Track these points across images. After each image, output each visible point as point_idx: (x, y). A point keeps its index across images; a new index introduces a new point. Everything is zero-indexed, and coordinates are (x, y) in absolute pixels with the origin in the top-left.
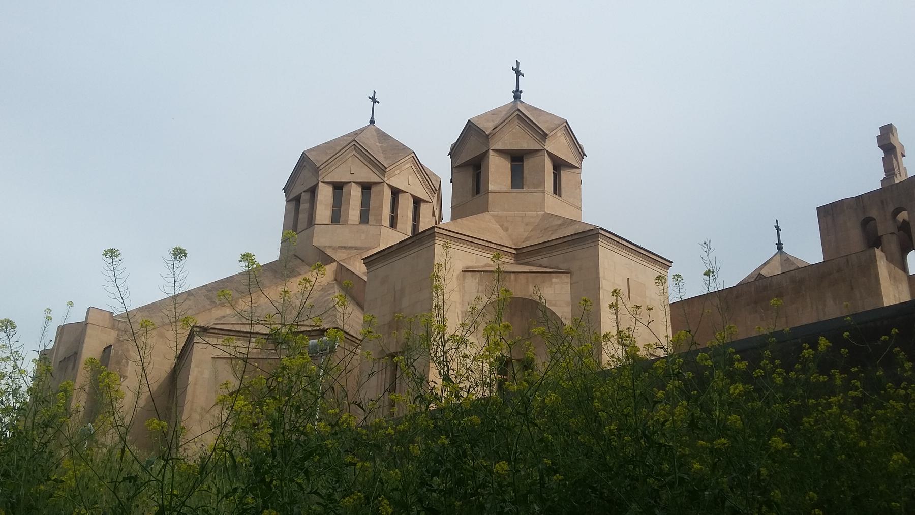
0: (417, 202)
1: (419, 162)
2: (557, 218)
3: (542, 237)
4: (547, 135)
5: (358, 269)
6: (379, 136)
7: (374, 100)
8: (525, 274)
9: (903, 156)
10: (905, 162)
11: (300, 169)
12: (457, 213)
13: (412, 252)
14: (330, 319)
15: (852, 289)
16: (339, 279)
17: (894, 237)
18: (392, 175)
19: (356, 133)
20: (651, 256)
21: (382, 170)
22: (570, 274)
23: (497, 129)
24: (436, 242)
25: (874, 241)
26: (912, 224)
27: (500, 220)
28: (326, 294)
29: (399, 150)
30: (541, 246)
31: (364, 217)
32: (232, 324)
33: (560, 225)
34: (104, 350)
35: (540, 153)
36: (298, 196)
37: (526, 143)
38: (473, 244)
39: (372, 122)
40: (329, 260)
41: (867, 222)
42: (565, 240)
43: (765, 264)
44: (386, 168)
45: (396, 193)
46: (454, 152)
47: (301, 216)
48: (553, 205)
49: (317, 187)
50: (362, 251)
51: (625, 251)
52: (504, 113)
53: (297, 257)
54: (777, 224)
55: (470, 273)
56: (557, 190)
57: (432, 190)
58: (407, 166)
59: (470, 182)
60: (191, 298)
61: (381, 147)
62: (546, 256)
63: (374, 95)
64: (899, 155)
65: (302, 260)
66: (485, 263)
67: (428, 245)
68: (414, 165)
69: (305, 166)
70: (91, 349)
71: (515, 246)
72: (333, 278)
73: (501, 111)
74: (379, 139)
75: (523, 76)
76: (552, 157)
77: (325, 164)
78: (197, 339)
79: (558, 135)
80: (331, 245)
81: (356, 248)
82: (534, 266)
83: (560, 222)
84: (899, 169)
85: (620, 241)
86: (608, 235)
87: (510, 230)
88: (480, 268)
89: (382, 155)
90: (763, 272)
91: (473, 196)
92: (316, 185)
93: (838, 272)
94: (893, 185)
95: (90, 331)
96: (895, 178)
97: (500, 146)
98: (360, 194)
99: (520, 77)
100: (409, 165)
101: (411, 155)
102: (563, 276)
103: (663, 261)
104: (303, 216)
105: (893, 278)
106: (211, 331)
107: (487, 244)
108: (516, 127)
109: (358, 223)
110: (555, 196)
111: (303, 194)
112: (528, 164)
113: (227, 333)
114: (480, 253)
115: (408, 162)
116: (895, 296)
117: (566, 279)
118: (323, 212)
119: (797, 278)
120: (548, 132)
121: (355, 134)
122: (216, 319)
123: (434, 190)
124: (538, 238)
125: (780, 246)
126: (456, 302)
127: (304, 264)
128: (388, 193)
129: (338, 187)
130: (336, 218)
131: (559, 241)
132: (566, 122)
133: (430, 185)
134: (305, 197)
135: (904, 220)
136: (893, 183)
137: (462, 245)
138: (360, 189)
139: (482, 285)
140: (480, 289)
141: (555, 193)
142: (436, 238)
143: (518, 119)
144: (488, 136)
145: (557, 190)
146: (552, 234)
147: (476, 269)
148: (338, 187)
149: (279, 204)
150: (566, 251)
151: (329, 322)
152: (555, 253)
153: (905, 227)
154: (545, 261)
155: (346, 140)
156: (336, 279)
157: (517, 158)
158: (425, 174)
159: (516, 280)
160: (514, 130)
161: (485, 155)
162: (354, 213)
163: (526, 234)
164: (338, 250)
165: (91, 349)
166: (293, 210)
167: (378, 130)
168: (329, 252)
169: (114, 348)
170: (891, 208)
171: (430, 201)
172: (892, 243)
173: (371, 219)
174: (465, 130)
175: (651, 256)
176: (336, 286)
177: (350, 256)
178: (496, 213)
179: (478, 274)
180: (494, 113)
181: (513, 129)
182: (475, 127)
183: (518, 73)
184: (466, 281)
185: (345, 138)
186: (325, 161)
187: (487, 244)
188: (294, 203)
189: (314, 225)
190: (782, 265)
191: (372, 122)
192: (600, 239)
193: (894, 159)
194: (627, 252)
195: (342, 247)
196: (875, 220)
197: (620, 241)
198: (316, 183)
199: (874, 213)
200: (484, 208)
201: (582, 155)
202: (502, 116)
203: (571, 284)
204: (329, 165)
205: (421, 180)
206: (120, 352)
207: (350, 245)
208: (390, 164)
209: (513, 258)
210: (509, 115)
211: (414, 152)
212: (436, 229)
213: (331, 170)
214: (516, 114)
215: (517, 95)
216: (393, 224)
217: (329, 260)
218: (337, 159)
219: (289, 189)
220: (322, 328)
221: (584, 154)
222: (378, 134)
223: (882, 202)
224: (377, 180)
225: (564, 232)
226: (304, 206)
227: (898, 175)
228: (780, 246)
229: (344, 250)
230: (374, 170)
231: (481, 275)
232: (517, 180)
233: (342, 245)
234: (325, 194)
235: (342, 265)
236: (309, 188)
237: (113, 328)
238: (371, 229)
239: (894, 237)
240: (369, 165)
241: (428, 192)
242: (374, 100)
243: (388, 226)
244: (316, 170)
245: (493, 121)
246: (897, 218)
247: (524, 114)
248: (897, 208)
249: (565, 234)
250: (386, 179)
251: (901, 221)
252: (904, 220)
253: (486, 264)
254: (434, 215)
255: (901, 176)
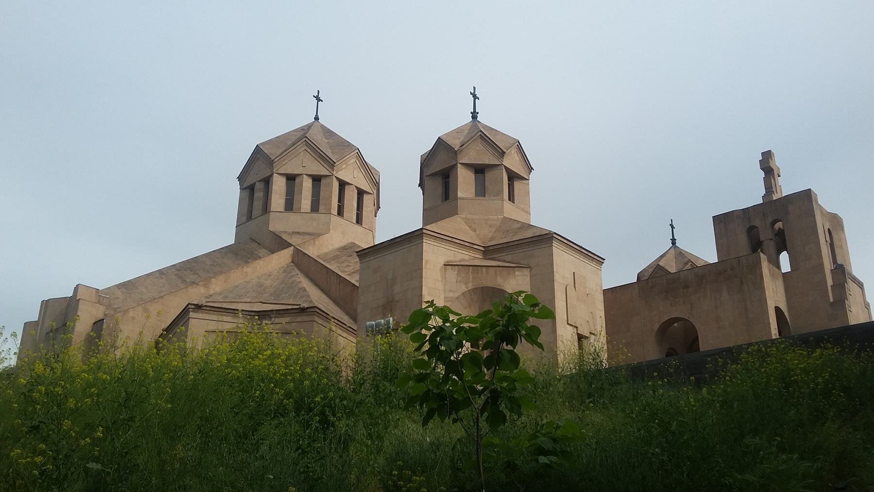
0: (361, 193)
1: (364, 159)
2: (515, 222)
3: (505, 237)
4: (504, 153)
5: (311, 252)
6: (325, 132)
7: (318, 99)
8: (494, 268)
9: (779, 176)
10: (780, 181)
11: (254, 161)
12: (430, 214)
13: (404, 247)
14: (304, 299)
15: (742, 283)
16: (296, 263)
17: (772, 242)
18: (340, 169)
19: (302, 129)
20: (590, 254)
21: (332, 165)
22: (529, 269)
23: (464, 146)
24: (424, 240)
25: (756, 246)
26: (786, 233)
27: (469, 223)
28: (290, 275)
29: (345, 147)
30: (505, 245)
31: (315, 208)
32: (221, 302)
33: (520, 228)
34: (94, 323)
35: (499, 167)
36: (252, 184)
37: (488, 159)
38: (452, 243)
39: (317, 118)
40: (285, 245)
41: (752, 231)
42: (525, 241)
43: (662, 256)
44: (335, 163)
45: (343, 184)
46: (426, 161)
47: (256, 203)
48: (510, 210)
49: (271, 179)
50: (315, 237)
51: (571, 251)
52: (466, 131)
53: (255, 241)
54: (672, 223)
55: (450, 266)
56: (511, 198)
57: (375, 184)
58: (353, 161)
59: (440, 190)
60: (163, 276)
61: (328, 143)
62: (510, 253)
63: (318, 94)
64: (776, 175)
65: (258, 243)
66: (461, 258)
67: (417, 243)
68: (359, 161)
69: (258, 158)
70: (83, 325)
71: (483, 244)
72: (290, 260)
73: (463, 130)
74: (324, 135)
75: (479, 99)
76: (507, 169)
77: (280, 157)
78: (192, 315)
79: (513, 153)
80: (285, 231)
81: (309, 234)
82: (499, 261)
83: (519, 225)
84: (776, 187)
85: (568, 243)
86: (559, 238)
87: (477, 231)
88: (456, 262)
89: (330, 150)
90: (661, 263)
91: (442, 201)
92: (271, 175)
93: (731, 270)
94: (770, 201)
95: (82, 306)
96: (773, 195)
97: (466, 161)
98: (311, 185)
99: (477, 100)
100: (354, 160)
101: (356, 152)
102: (525, 270)
103: (598, 259)
104: (258, 204)
105: (773, 275)
106: (204, 308)
107: (462, 243)
108: (479, 146)
109: (309, 211)
110: (509, 202)
111: (257, 183)
112: (489, 176)
113: (217, 310)
114: (457, 250)
115: (353, 158)
116: (773, 289)
117: (526, 272)
118: (278, 200)
119: (700, 274)
120: (505, 151)
121: (302, 130)
122: (206, 297)
123: (376, 183)
124: (502, 238)
125: (673, 241)
126: (440, 290)
127: (261, 247)
128: (336, 185)
129: (291, 179)
130: (290, 205)
131: (520, 242)
132: (519, 142)
133: (372, 179)
134: (259, 186)
135: (779, 228)
136: (771, 200)
137: (443, 243)
138: (310, 181)
139: (460, 276)
140: (458, 280)
141: (509, 200)
142: (424, 238)
143: (481, 139)
144: (456, 152)
145: (511, 198)
146: (513, 235)
147: (455, 262)
148: (291, 179)
149: (233, 192)
150: (526, 250)
151: (305, 301)
152: (517, 252)
153: (780, 234)
154: (509, 258)
155: (295, 136)
156: (293, 262)
157: (479, 170)
158: (366, 167)
159: (487, 271)
160: (478, 148)
161: (454, 167)
162: (305, 201)
163: (491, 235)
164: (293, 236)
165: (83, 325)
166: (247, 198)
167: (323, 127)
168: (285, 237)
169: (106, 322)
170: (770, 220)
171: (372, 193)
172: (770, 246)
173: (322, 208)
174: (435, 146)
175: (590, 254)
176: (294, 266)
177: (304, 241)
178: (464, 216)
179: (457, 267)
180: (458, 131)
181: (477, 147)
182: (444, 143)
183: (475, 97)
184: (447, 272)
185: (294, 133)
186: (278, 154)
187: (462, 243)
188: (247, 193)
189: (270, 212)
190: (676, 258)
191: (317, 118)
192: (554, 242)
193: (772, 180)
194: (573, 252)
195: (296, 232)
196: (757, 227)
197: (568, 243)
198: (269, 174)
199: (757, 223)
200: (454, 212)
201: (531, 169)
202: (465, 134)
203: (530, 277)
204: (281, 160)
205: (364, 173)
206: (111, 325)
207: (301, 231)
208: (338, 159)
209: (481, 254)
210: (473, 135)
211: (358, 149)
212: (424, 230)
213: (284, 163)
214: (479, 134)
215: (474, 115)
216: (340, 213)
217: (285, 245)
218: (291, 152)
219: (243, 180)
220: (302, 306)
221: (532, 168)
222: (323, 130)
223: (764, 214)
224: (327, 173)
225: (524, 235)
226: (259, 194)
227: (775, 192)
228: (673, 241)
229: (298, 236)
230: (323, 163)
231: (459, 268)
232: (481, 191)
233: (297, 231)
234: (279, 185)
235: (298, 249)
236: (264, 178)
237: (99, 302)
238: (321, 217)
239: (772, 241)
240: (319, 160)
241: (371, 187)
242: (318, 99)
243: (336, 214)
244: (271, 163)
245: (458, 139)
246: (775, 227)
247: (486, 136)
248: (775, 220)
249: (524, 236)
250: (334, 172)
251: (777, 229)
252: (779, 228)
253: (462, 259)
254: (374, 206)
255: (777, 193)
